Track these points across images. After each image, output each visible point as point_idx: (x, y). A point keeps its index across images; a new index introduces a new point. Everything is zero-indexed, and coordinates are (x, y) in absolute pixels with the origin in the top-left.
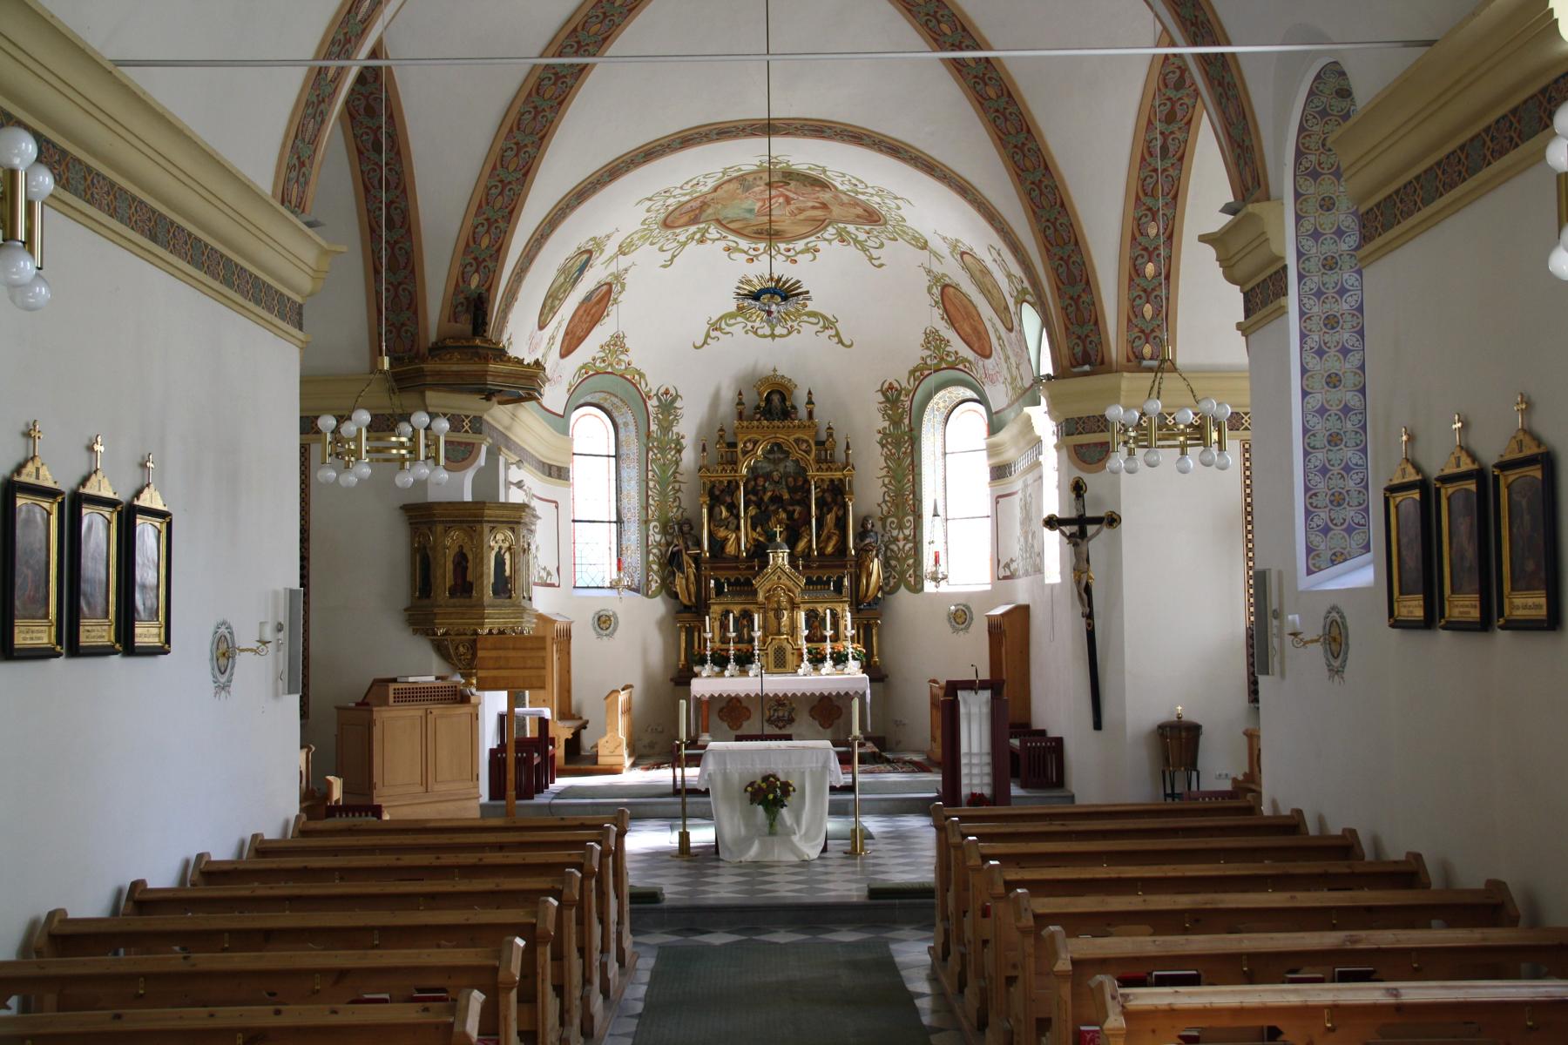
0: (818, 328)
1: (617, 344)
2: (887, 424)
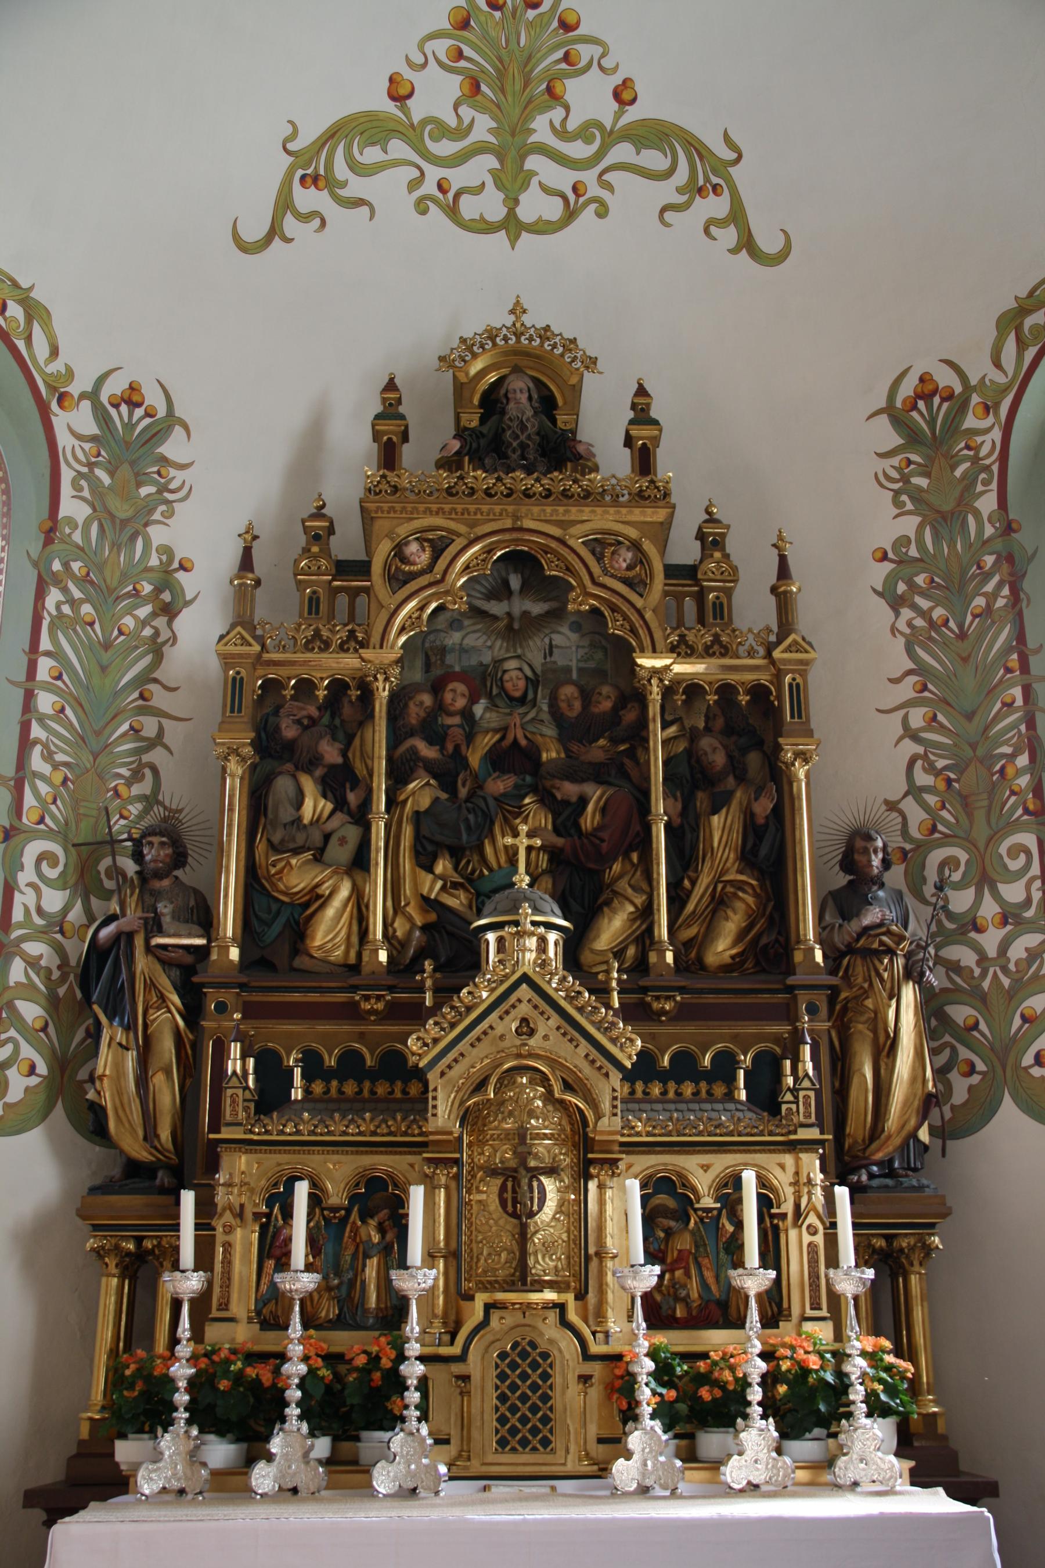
0: (667, 192)
2: (909, 525)
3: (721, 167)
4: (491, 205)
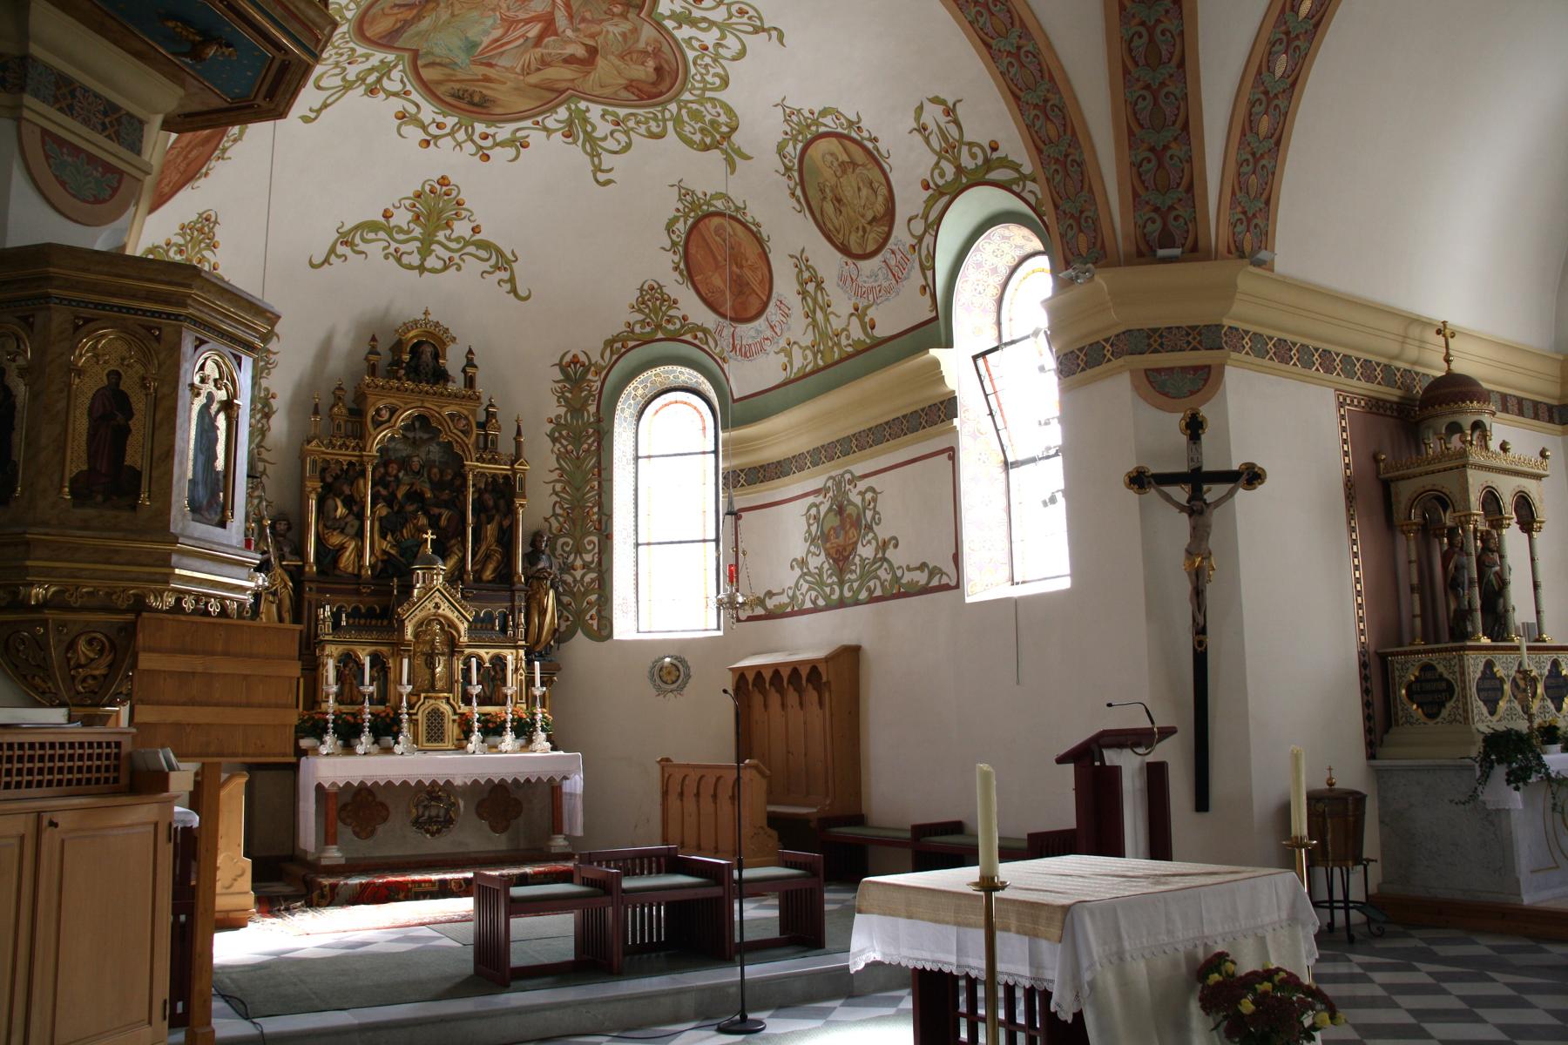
0: (486, 266)
1: (203, 229)
2: (562, 411)
3: (508, 262)
4: (415, 260)
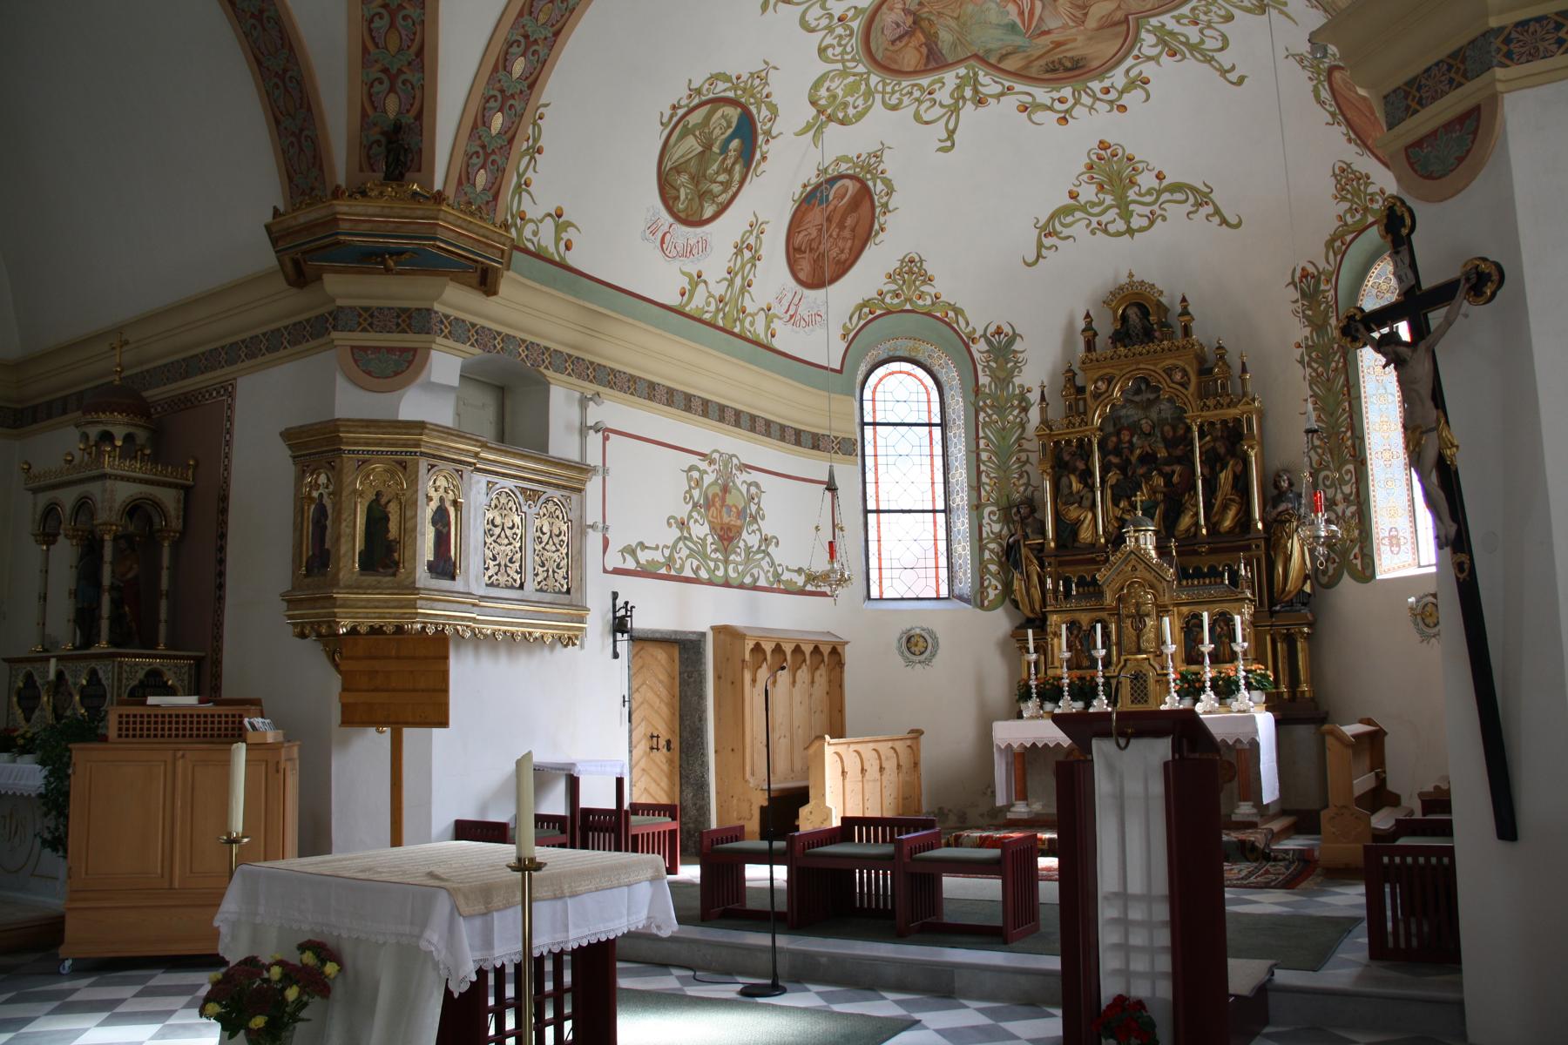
0: (1188, 207)
1: (912, 270)
3: (1206, 195)
